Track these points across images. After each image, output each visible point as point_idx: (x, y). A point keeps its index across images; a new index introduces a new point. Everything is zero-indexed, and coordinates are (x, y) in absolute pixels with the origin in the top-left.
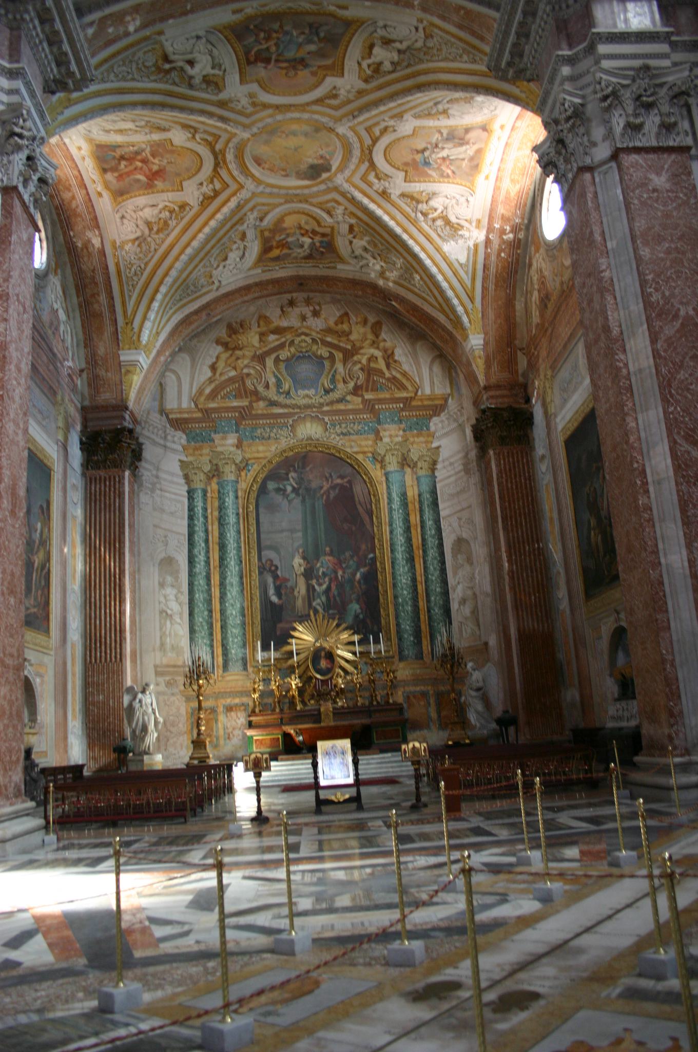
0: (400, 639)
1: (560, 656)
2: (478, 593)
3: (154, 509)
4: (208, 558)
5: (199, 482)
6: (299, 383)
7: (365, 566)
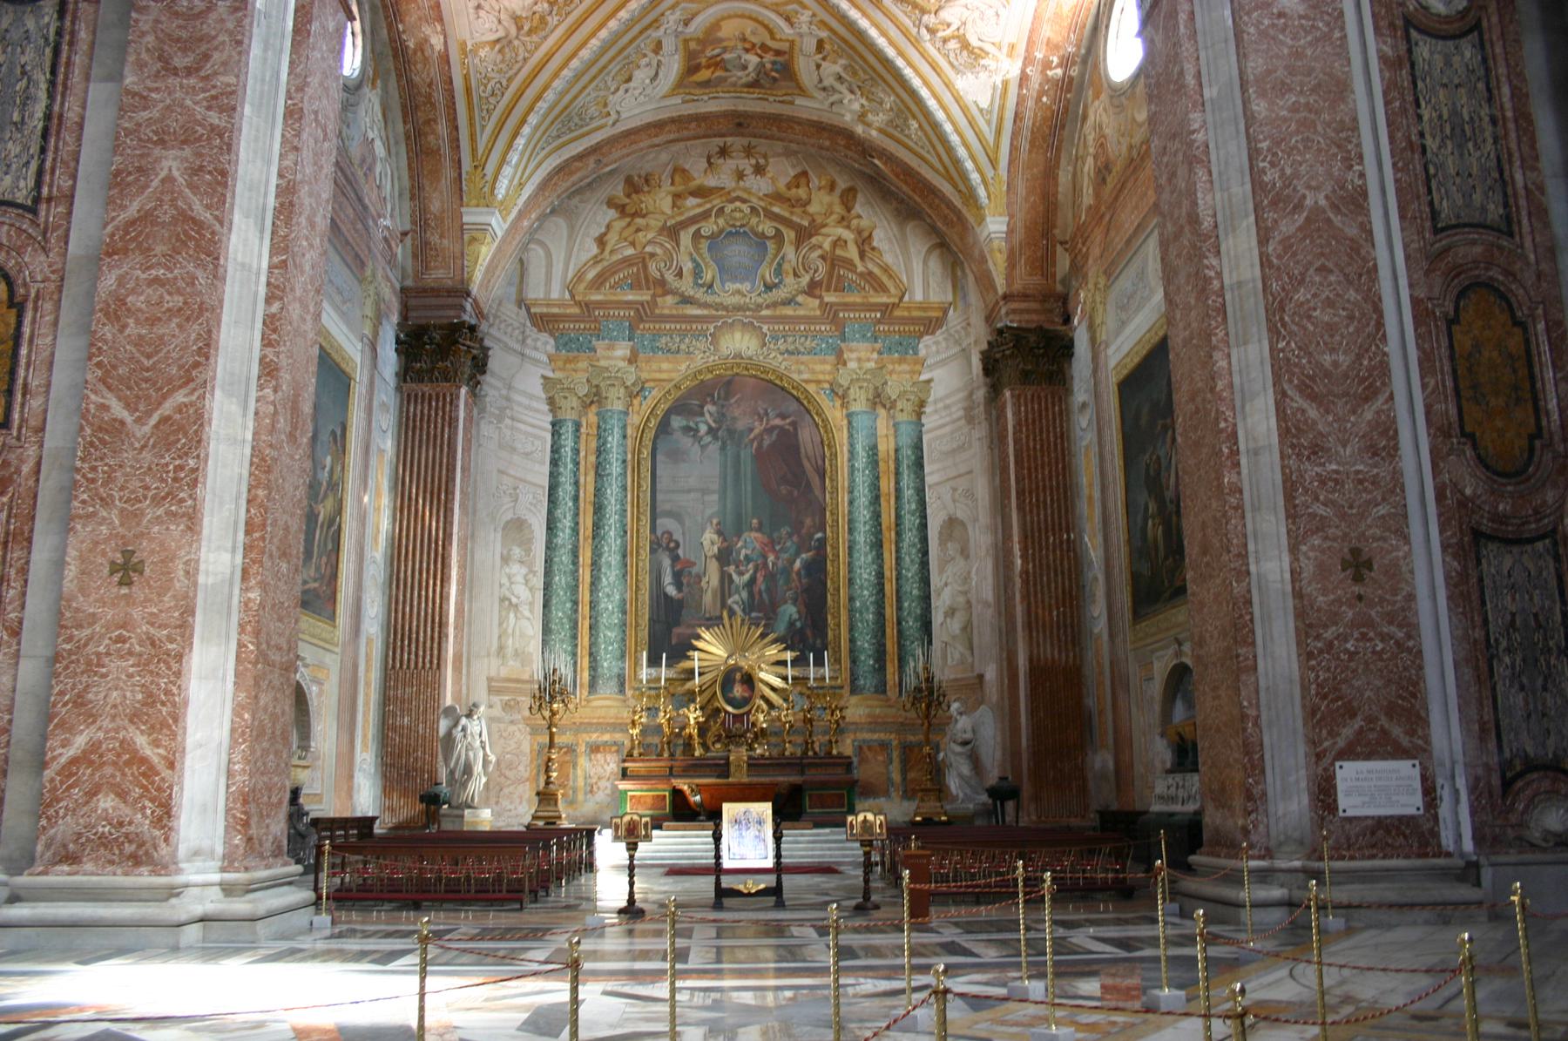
0: (854, 661)
1: (1090, 702)
2: (974, 602)
3: (501, 446)
4: (577, 524)
6: (726, 272)
7: (809, 550)
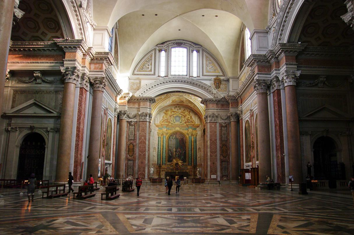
0: (189, 162)
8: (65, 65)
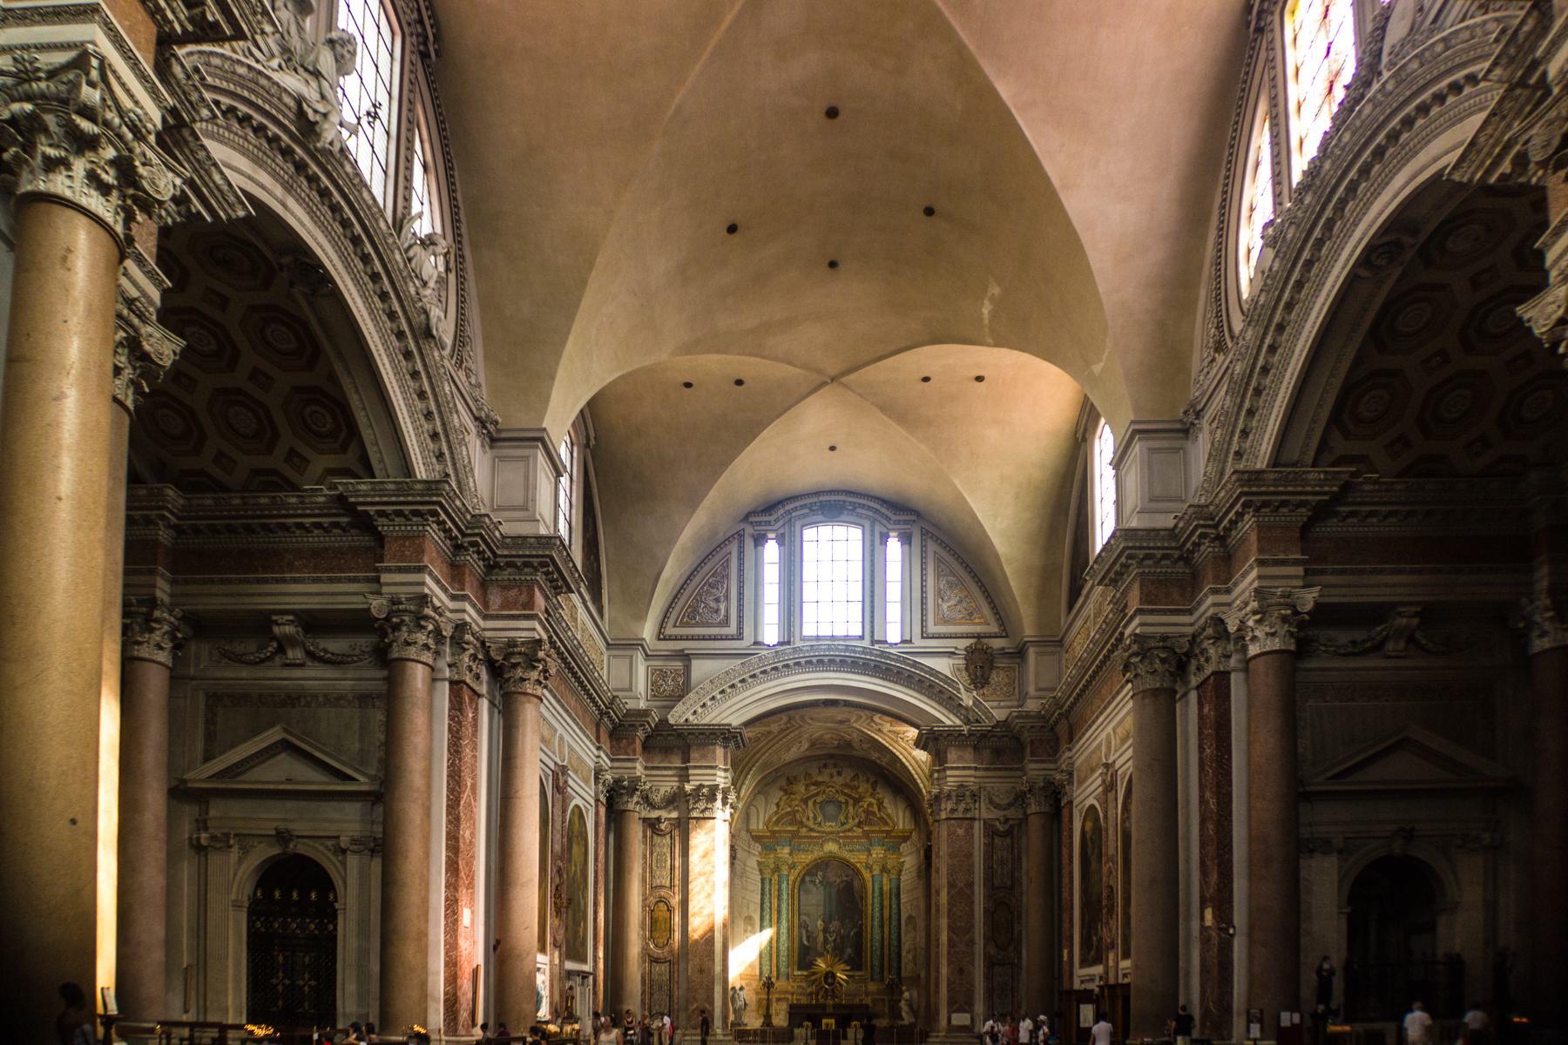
5: (768, 873)
6: (827, 818)
8: (385, 589)
